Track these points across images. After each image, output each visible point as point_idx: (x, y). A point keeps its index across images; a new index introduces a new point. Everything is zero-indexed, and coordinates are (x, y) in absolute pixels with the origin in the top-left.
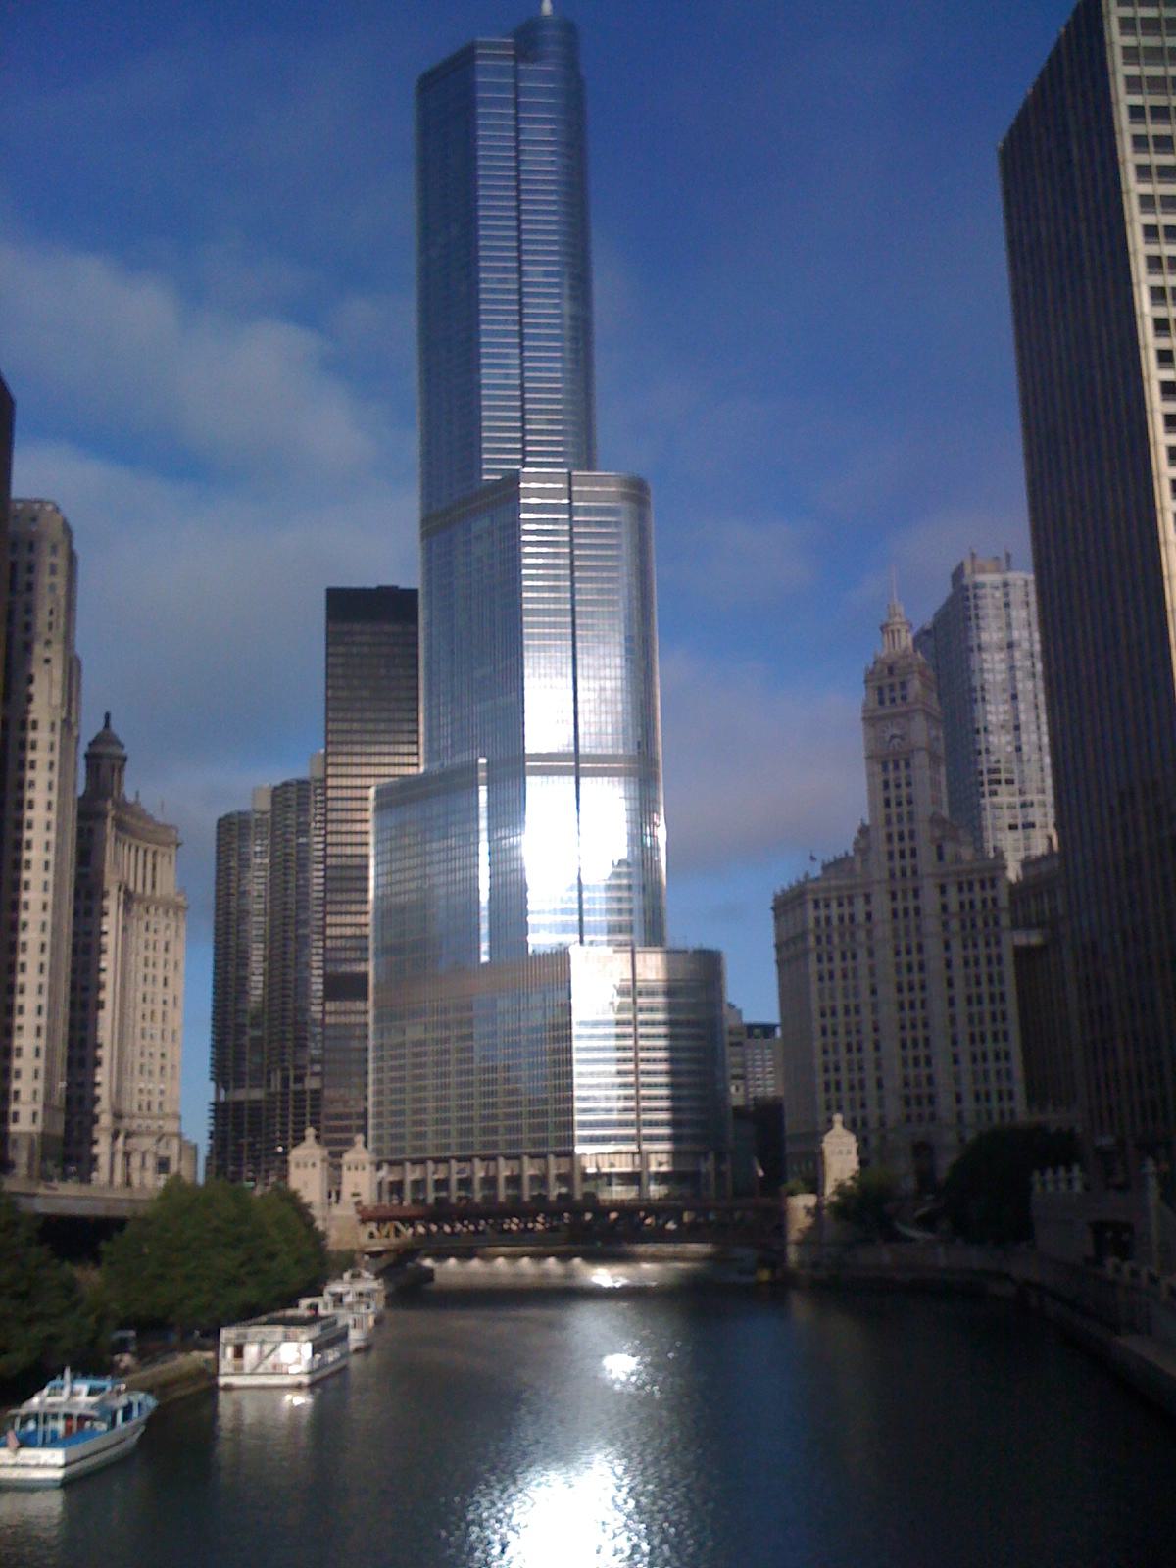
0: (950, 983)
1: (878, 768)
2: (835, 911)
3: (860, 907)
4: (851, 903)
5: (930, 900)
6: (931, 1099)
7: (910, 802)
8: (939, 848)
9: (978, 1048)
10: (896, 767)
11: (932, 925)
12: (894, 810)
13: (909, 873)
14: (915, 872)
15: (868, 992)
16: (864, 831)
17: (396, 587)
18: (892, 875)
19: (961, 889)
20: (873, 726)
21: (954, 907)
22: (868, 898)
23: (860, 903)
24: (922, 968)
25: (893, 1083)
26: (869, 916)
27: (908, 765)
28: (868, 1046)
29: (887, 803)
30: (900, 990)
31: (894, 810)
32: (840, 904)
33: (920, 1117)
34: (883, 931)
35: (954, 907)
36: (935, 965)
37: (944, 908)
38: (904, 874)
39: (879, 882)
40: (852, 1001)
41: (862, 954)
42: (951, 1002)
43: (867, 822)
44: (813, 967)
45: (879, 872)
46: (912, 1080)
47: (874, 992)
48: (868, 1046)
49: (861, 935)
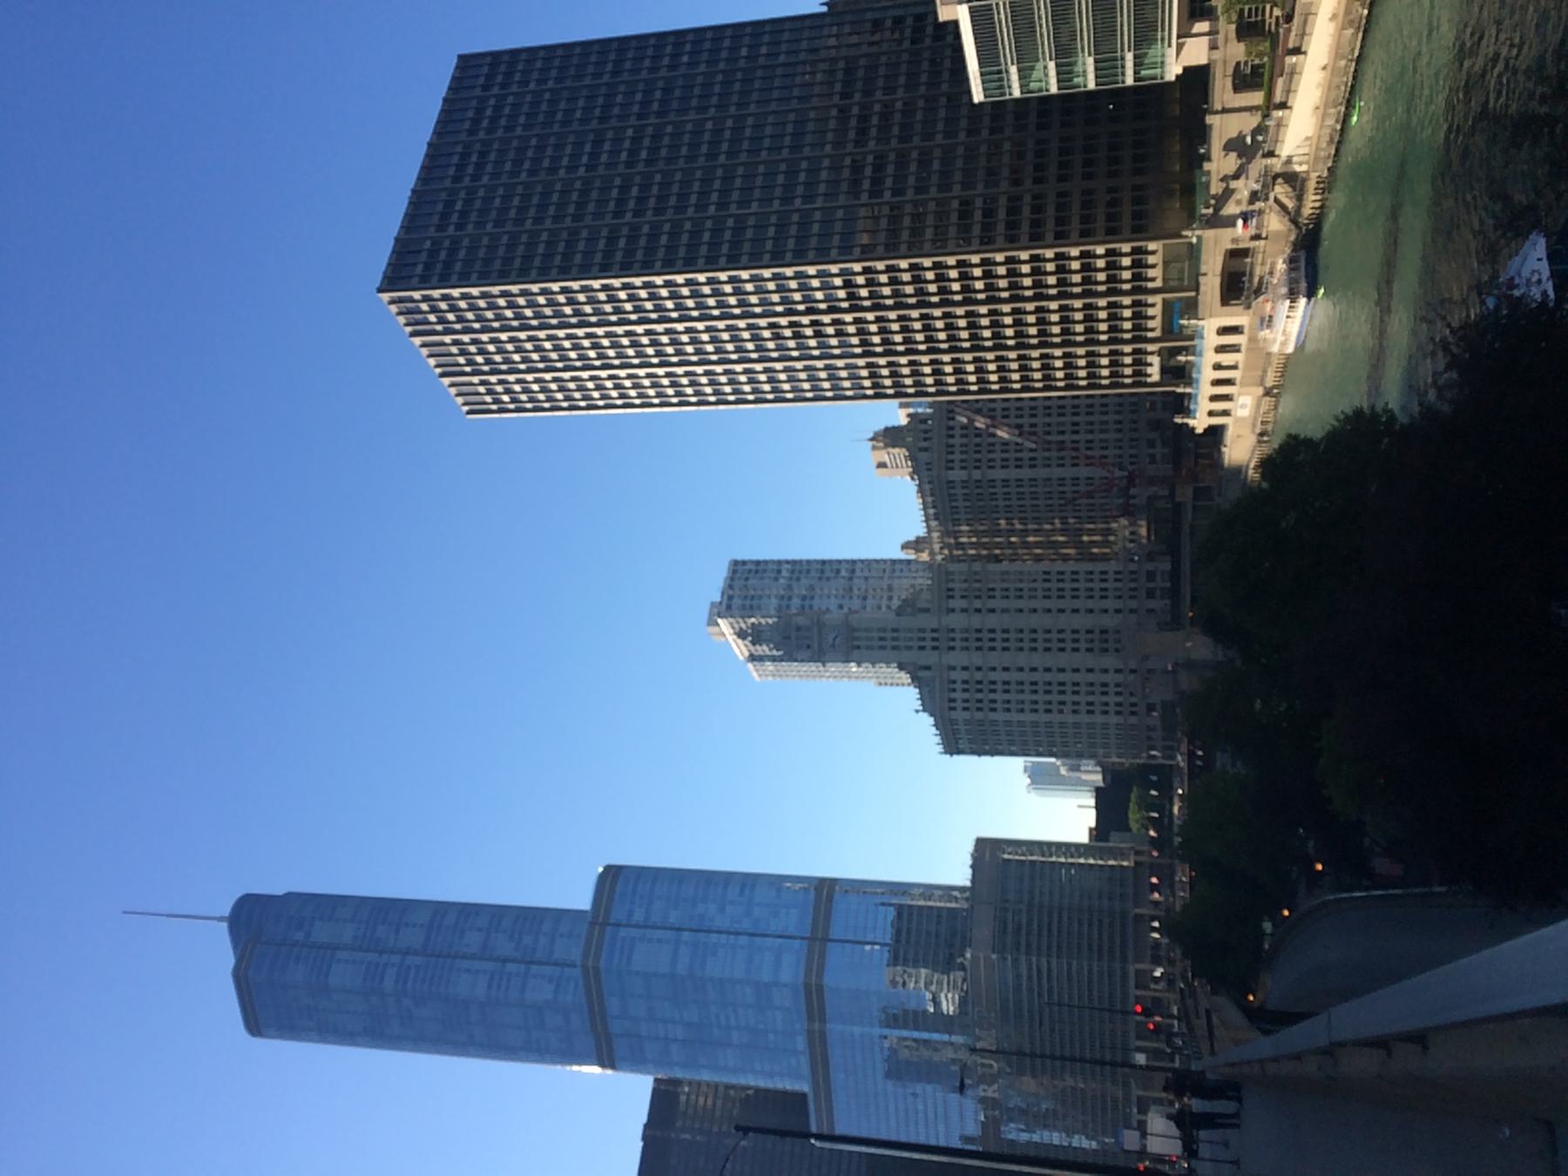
1: (856, 652)
2: (958, 695)
3: (958, 675)
5: (956, 621)
6: (1103, 632)
9: (1068, 594)
17: (647, 1127)
23: (954, 675)
25: (1090, 660)
26: (965, 669)
28: (1062, 677)
29: (883, 648)
32: (954, 690)
35: (963, 603)
36: (1006, 621)
37: (964, 610)
39: (940, 657)
41: (993, 676)
44: (1000, 716)
47: (1021, 669)
48: (1062, 677)
49: (978, 676)
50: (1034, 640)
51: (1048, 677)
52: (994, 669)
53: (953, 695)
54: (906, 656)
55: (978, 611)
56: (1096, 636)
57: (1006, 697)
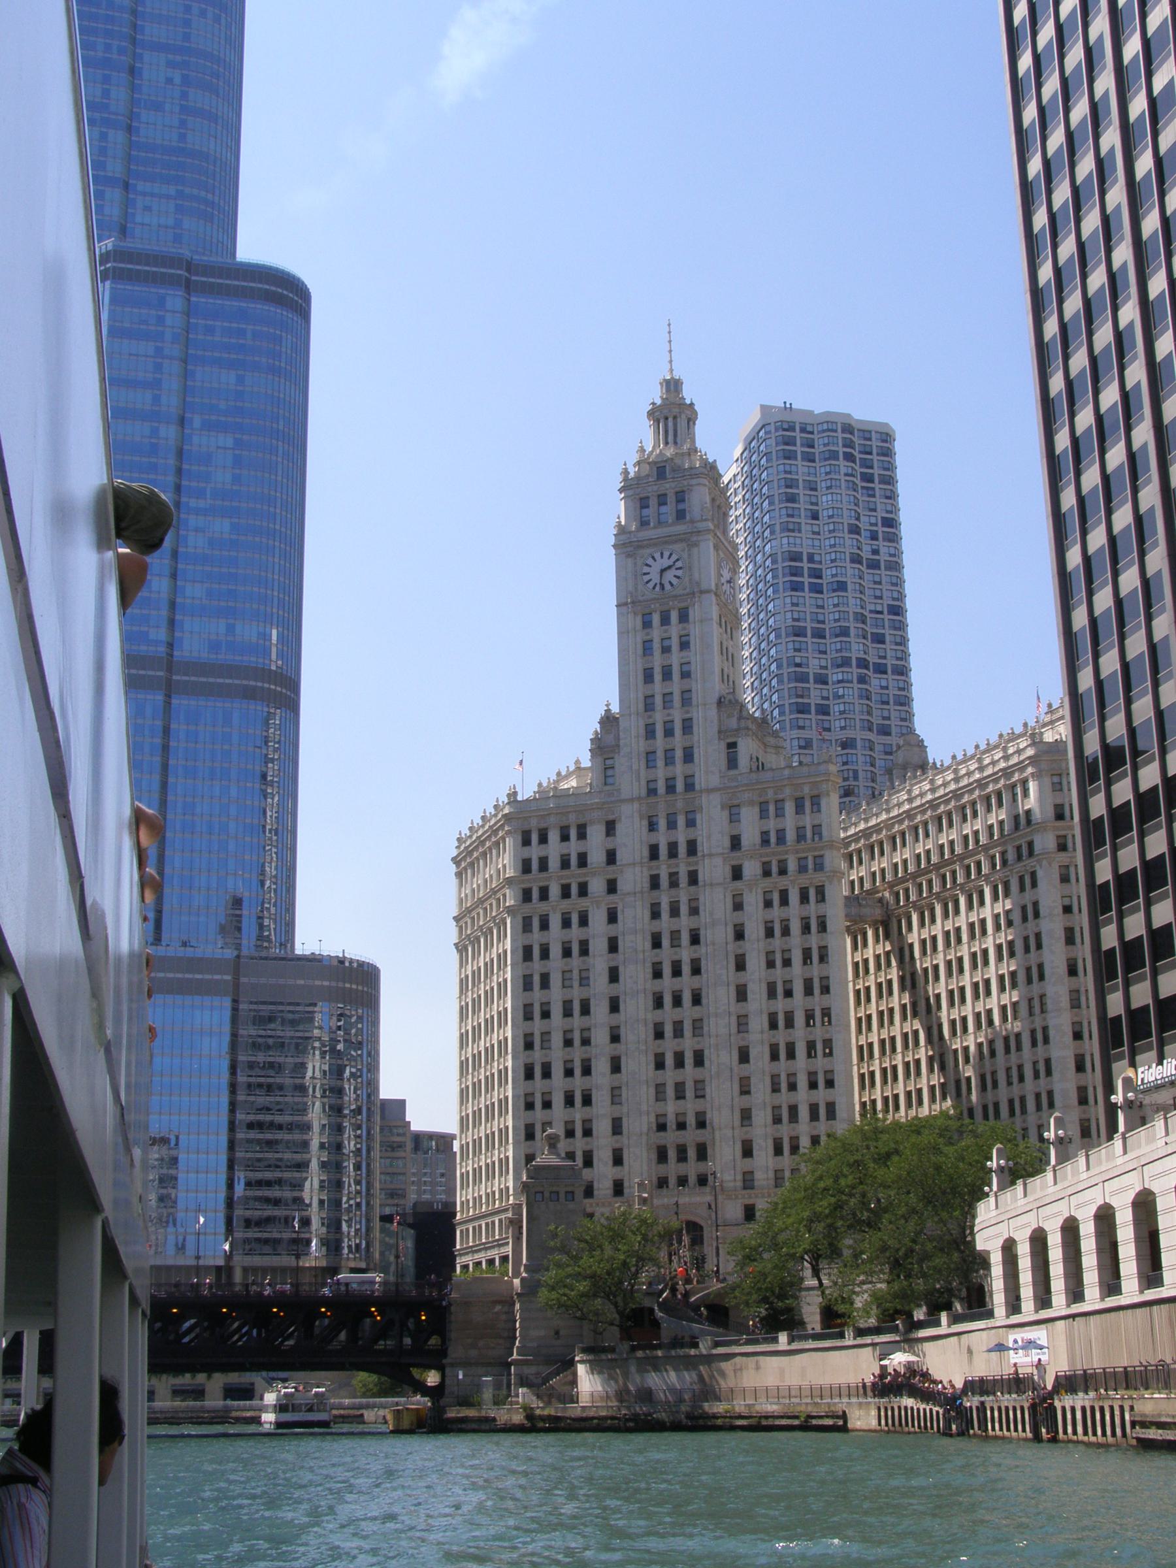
0: (741, 965)
4: (582, 835)
6: (702, 1153)
7: (686, 675)
8: (732, 746)
10: (665, 620)
11: (713, 869)
12: (658, 687)
13: (680, 786)
14: (689, 786)
15: (605, 978)
16: (608, 721)
18: (652, 792)
19: (764, 814)
20: (629, 556)
21: (750, 835)
22: (611, 828)
23: (596, 834)
24: (695, 939)
25: (639, 1125)
26: (611, 857)
27: (684, 617)
28: (601, 1067)
29: (648, 677)
30: (657, 974)
31: (658, 687)
32: (565, 838)
33: (682, 1181)
34: (633, 878)
36: (717, 936)
38: (671, 788)
39: (632, 800)
40: (576, 994)
41: (598, 918)
42: (742, 994)
43: (615, 709)
45: (630, 783)
46: (671, 1121)
50: (677, 1001)
51: (600, 1037)
52: (612, 917)
53: (554, 836)
54: (632, 731)
55: (737, 874)
56: (691, 1137)
57: (556, 951)
